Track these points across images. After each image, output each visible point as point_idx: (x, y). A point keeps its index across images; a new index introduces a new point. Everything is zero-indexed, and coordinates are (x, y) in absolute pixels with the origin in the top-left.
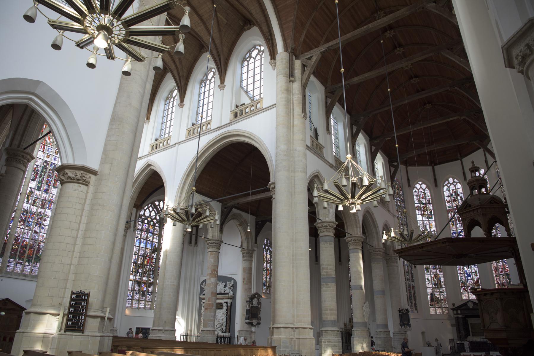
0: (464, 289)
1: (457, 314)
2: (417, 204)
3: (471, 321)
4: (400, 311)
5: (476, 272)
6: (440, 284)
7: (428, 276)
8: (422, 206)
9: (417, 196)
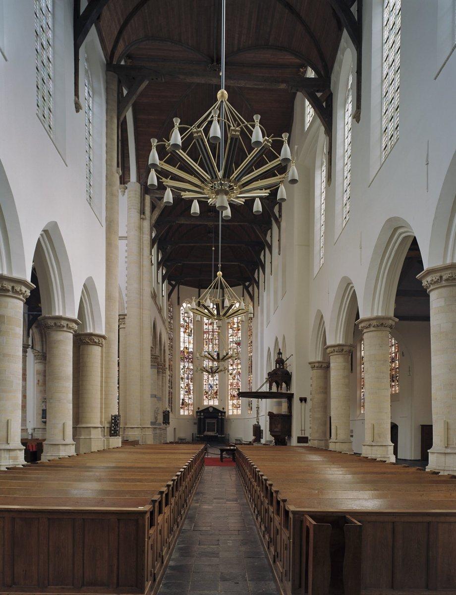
0: (206, 397)
1: (200, 415)
2: (182, 322)
3: (208, 421)
4: (164, 412)
5: (217, 384)
6: (190, 391)
7: (182, 385)
8: (185, 324)
9: (182, 314)
